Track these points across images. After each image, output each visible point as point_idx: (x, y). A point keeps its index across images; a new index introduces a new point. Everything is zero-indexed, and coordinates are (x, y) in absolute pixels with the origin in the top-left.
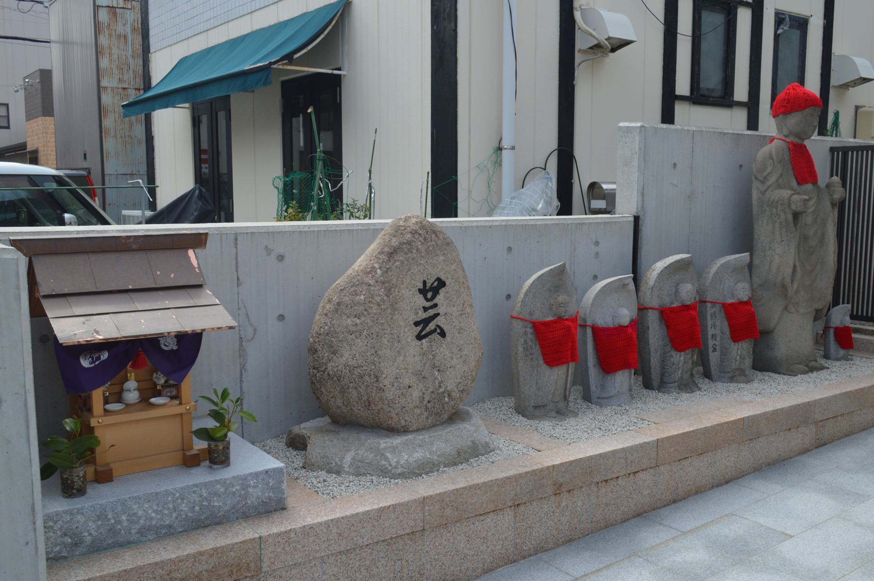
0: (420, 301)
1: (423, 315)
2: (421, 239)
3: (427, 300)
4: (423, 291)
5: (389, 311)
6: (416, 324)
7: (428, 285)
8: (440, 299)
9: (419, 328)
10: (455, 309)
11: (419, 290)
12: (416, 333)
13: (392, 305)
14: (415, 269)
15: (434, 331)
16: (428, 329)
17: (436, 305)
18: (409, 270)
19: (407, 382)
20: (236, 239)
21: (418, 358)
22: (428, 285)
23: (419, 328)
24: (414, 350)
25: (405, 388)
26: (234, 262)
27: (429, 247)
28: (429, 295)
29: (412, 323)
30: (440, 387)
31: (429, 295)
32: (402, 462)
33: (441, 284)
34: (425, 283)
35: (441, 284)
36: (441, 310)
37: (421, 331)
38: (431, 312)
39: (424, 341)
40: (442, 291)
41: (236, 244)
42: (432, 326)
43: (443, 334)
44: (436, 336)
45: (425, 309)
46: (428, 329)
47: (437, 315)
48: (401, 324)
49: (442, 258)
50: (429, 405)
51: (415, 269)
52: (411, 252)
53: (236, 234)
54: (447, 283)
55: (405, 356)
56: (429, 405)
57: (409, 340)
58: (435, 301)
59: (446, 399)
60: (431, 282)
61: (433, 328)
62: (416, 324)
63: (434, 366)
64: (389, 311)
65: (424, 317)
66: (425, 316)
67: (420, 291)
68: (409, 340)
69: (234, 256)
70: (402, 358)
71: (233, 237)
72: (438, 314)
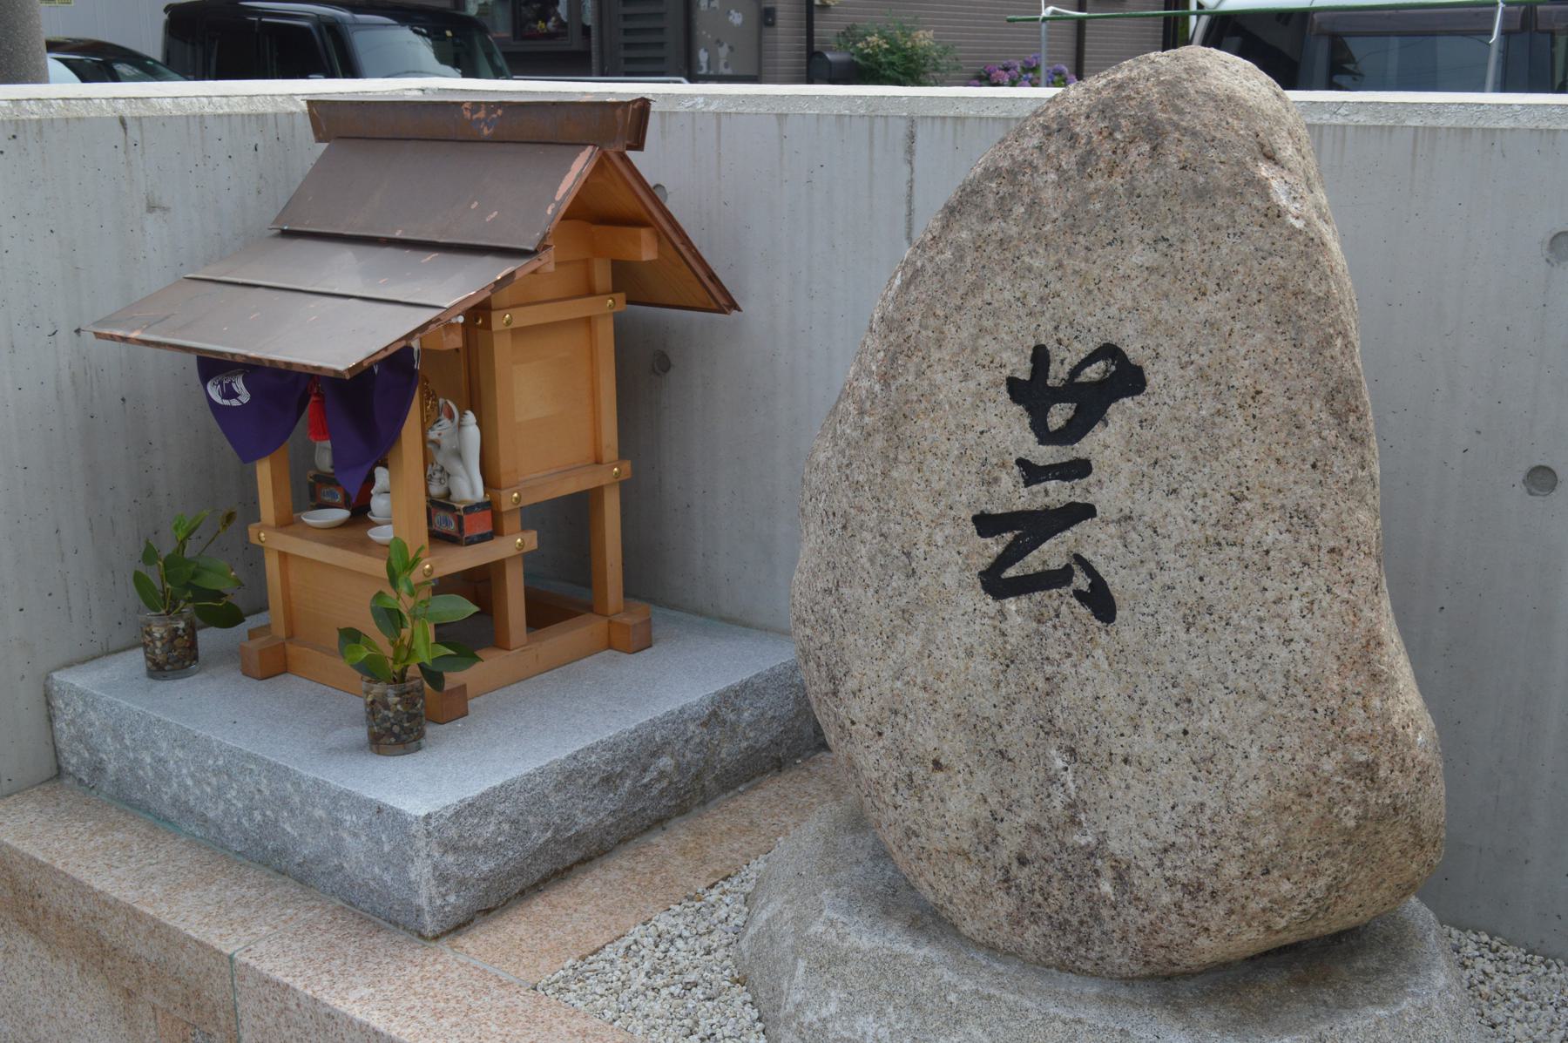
0: (1012, 432)
1: (1015, 496)
2: (1068, 161)
3: (1045, 436)
4: (1030, 393)
5: (879, 442)
6: (986, 524)
7: (1057, 374)
8: (1102, 445)
9: (995, 546)
10: (1174, 506)
11: (1013, 385)
12: (983, 562)
13: (891, 422)
14: (1002, 289)
15: (1061, 577)
16: (1032, 563)
17: (1080, 469)
18: (975, 288)
19: (927, 740)
20: (912, 137)
21: (983, 668)
22: (1057, 374)
23: (995, 546)
24: (970, 623)
25: (919, 760)
26: (904, 211)
27: (1088, 197)
28: (1058, 416)
29: (967, 514)
30: (1074, 821)
31: (1058, 416)
32: (809, 1017)
33: (1127, 378)
34: (1040, 357)
35: (1127, 378)
36: (1105, 493)
37: (1005, 560)
38: (1056, 493)
39: (1011, 604)
40: (1122, 412)
41: (910, 151)
42: (1052, 553)
43: (1100, 602)
44: (1061, 601)
45: (1032, 473)
46: (1032, 563)
47: (1085, 511)
48: (921, 505)
49: (1140, 256)
50: (1022, 875)
51: (1002, 289)
52: (1005, 214)
53: (912, 121)
54: (1153, 380)
55: (928, 640)
56: (1022, 875)
57: (949, 579)
58: (1084, 448)
59: (1106, 888)
60: (1073, 359)
61: (1056, 563)
62: (986, 524)
63: (1048, 727)
64: (879, 442)
65: (1018, 505)
66: (1026, 499)
67: (1016, 389)
68: (949, 579)
69: (905, 189)
70: (916, 641)
71: (901, 130)
72: (1087, 511)
